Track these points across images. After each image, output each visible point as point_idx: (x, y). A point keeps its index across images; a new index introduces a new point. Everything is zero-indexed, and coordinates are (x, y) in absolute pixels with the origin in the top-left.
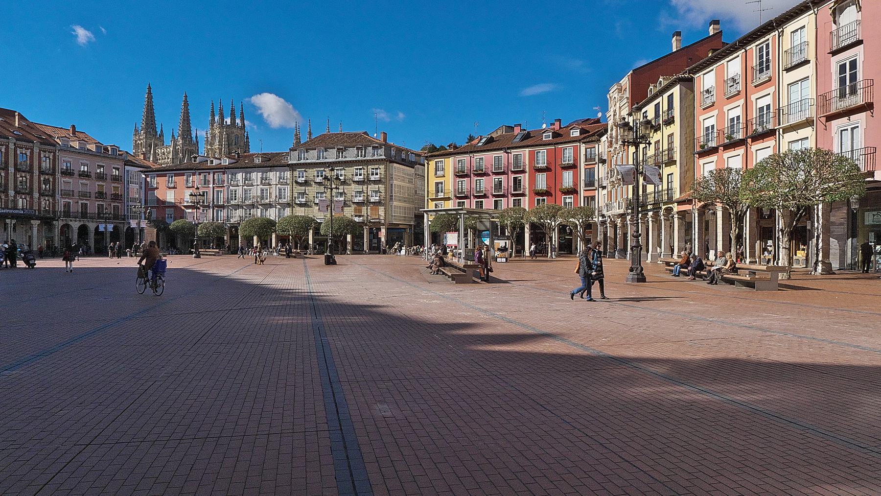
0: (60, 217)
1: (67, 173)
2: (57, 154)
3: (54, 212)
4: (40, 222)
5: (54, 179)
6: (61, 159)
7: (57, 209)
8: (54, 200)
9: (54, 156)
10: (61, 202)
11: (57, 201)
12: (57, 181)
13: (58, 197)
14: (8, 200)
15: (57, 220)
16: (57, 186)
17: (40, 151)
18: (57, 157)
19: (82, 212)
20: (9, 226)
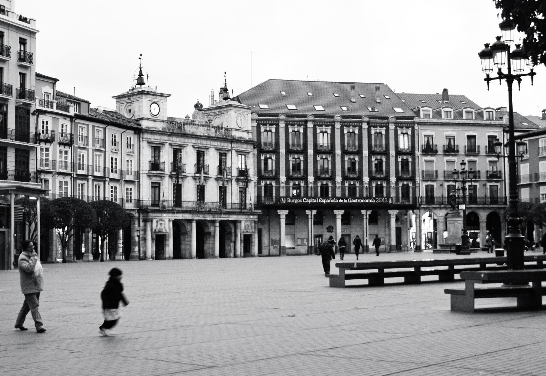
0: (421, 204)
1: (429, 150)
2: (416, 128)
3: (415, 198)
4: (398, 211)
5: (414, 159)
6: (421, 134)
7: (417, 195)
8: (414, 183)
9: (413, 132)
10: (422, 185)
11: (417, 185)
12: (417, 161)
13: (418, 179)
14: (363, 187)
15: (418, 208)
16: (417, 168)
17: (396, 127)
18: (416, 132)
19: (427, 196)
20: (365, 217)
